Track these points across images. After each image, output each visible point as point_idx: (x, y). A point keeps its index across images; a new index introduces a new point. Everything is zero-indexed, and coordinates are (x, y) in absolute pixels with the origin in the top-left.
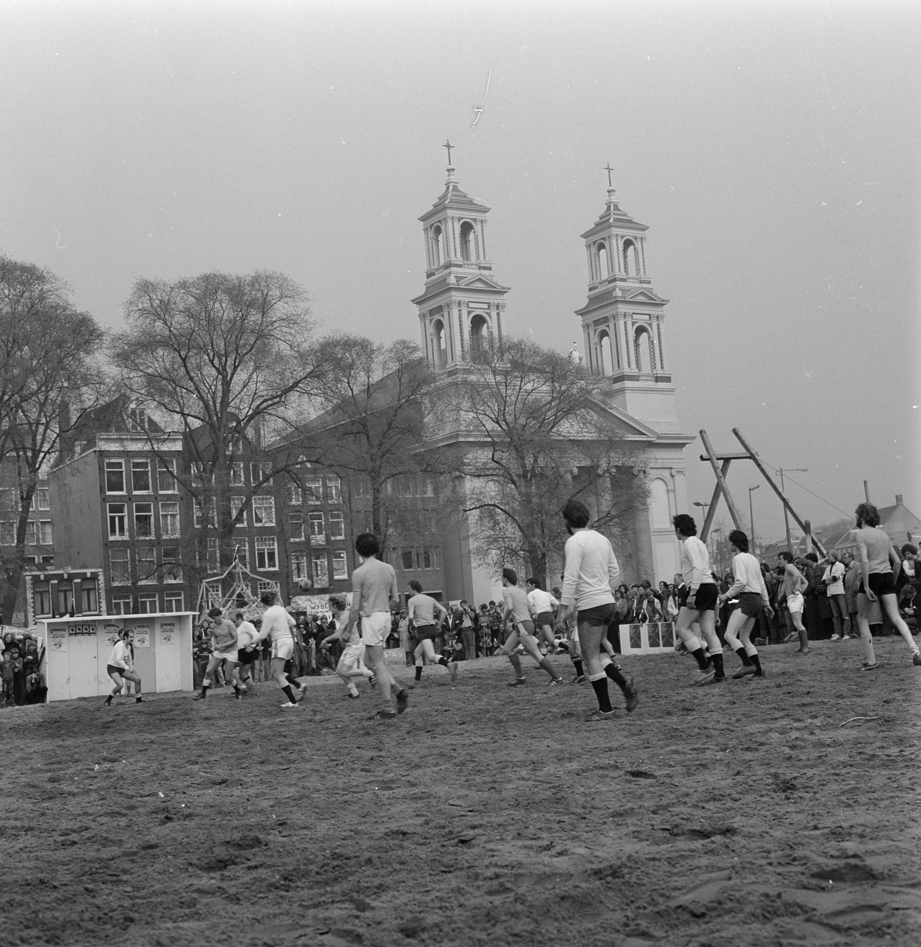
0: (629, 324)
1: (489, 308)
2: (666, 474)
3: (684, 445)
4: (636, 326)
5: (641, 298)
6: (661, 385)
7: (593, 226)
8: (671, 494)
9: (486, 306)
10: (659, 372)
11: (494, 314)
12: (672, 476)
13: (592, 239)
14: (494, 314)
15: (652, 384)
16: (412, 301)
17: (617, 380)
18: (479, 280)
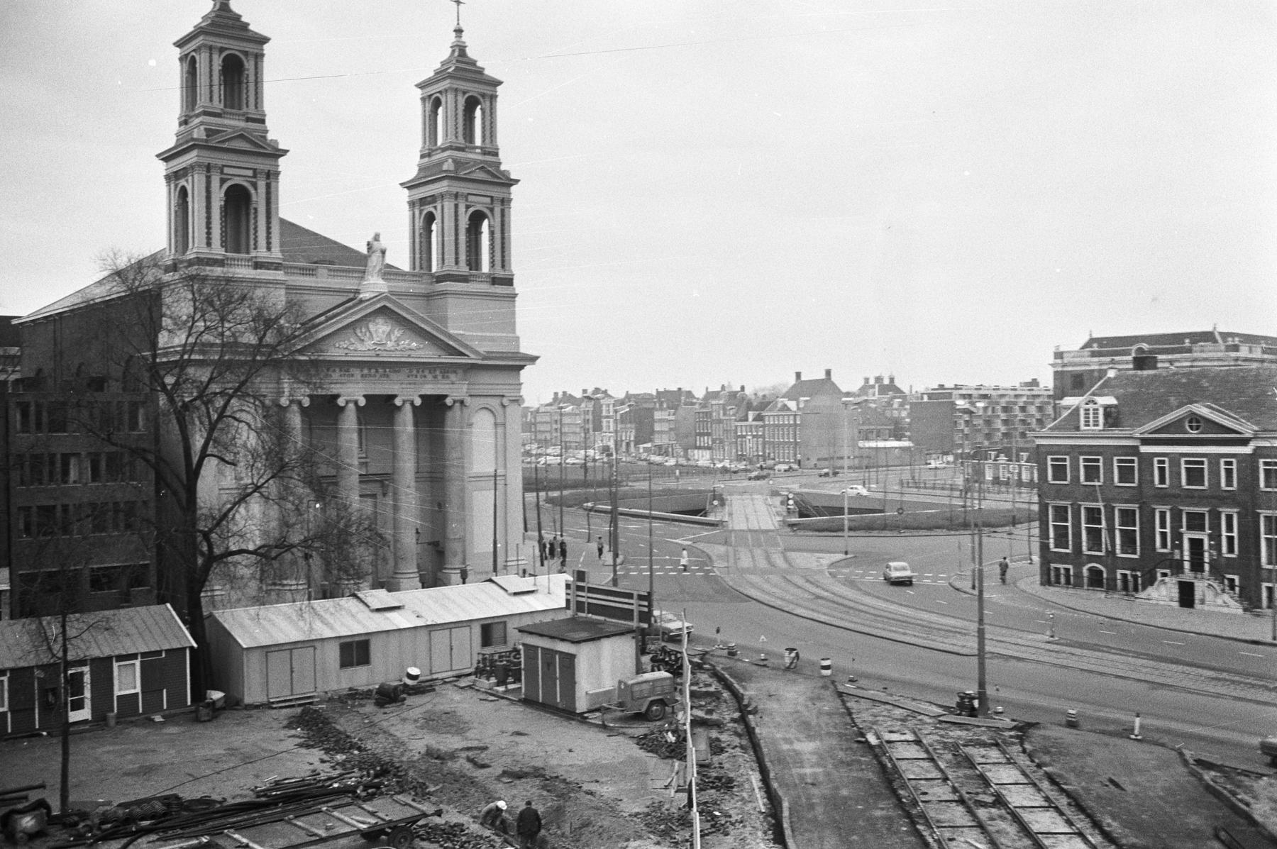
0: (462, 208)
1: (255, 176)
2: (494, 403)
3: (522, 367)
4: (471, 210)
5: (481, 175)
6: (499, 289)
7: (432, 74)
8: (500, 430)
9: (250, 173)
10: (499, 273)
11: (262, 184)
12: (504, 407)
13: (430, 90)
14: (262, 184)
15: (485, 287)
16: (158, 156)
17: (440, 279)
18: (242, 137)
